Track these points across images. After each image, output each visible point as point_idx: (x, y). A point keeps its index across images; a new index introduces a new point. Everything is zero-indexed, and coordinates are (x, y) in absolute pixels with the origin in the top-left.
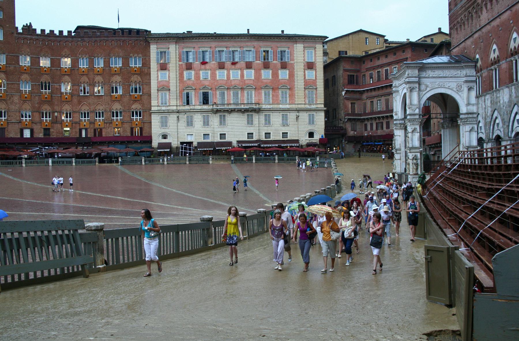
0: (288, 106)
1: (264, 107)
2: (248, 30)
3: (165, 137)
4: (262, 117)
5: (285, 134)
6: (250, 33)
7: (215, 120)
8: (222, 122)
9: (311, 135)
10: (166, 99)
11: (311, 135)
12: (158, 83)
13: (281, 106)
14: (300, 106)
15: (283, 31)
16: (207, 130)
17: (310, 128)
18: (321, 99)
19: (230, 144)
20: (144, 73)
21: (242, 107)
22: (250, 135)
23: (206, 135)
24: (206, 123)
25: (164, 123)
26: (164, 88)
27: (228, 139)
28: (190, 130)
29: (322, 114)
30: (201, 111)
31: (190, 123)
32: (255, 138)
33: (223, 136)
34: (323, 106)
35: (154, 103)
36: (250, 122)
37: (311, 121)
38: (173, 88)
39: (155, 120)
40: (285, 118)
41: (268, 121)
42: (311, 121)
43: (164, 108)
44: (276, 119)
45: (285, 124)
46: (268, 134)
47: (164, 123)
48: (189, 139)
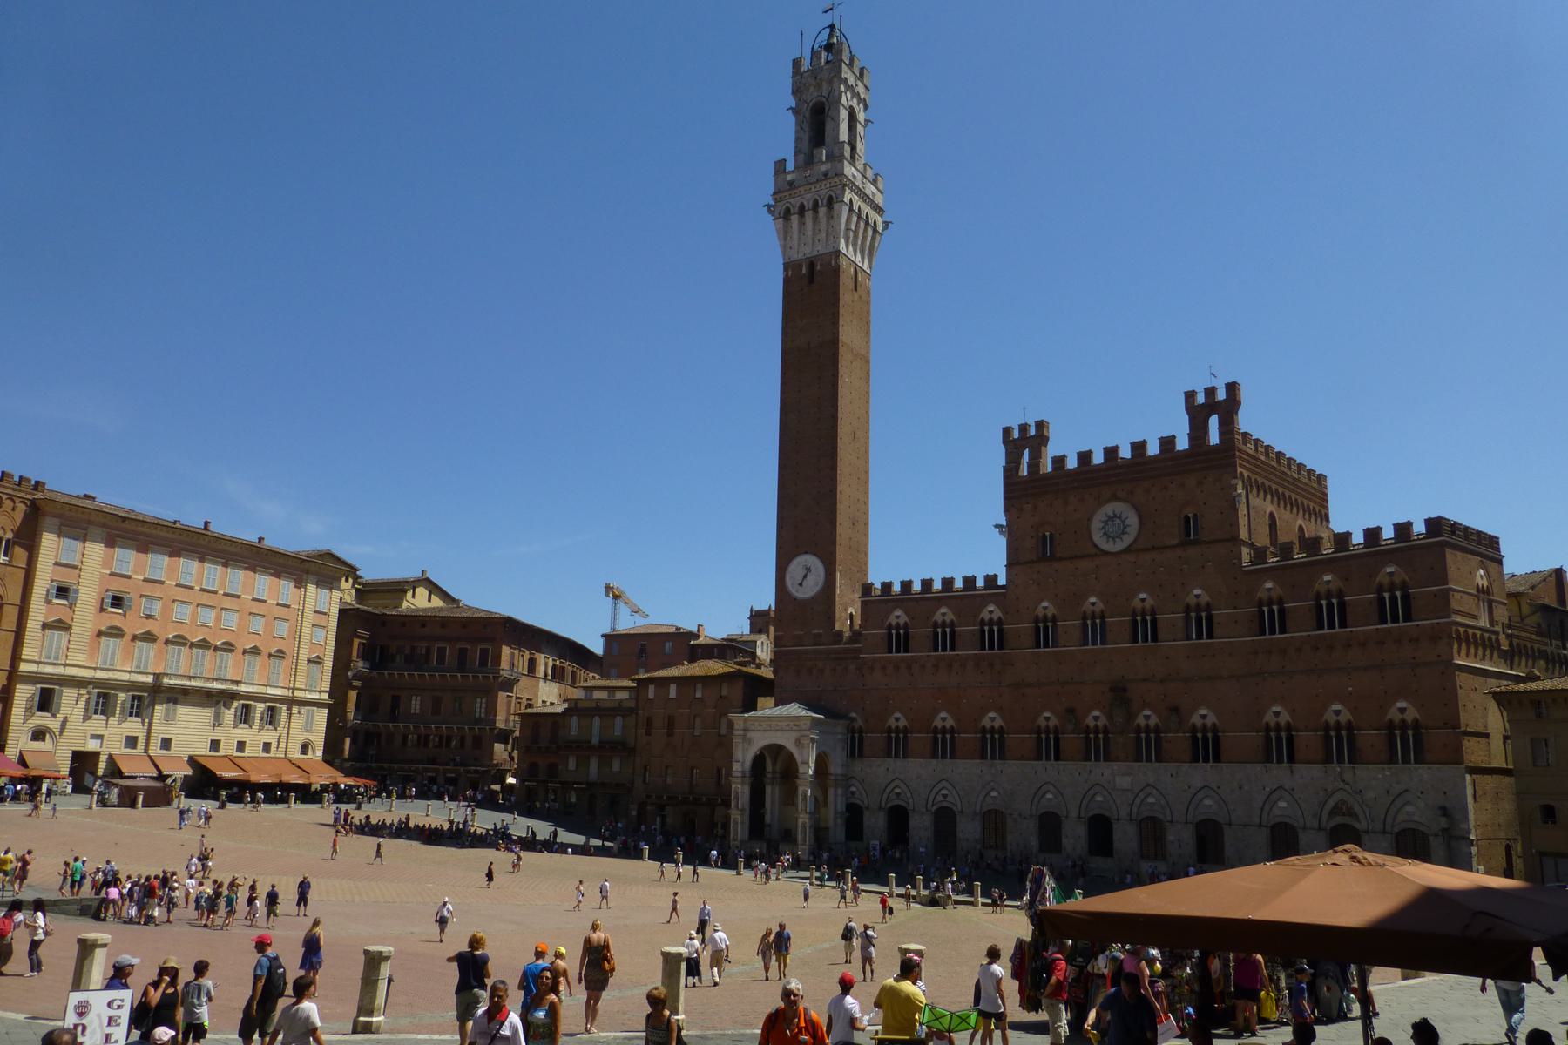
1: (243, 688)
2: (207, 523)
3: (39, 735)
6: (211, 527)
9: (305, 748)
10: (59, 648)
14: (297, 693)
15: (260, 540)
17: (307, 736)
18: (326, 686)
22: (215, 745)
23: (131, 742)
28: (97, 723)
29: (325, 711)
33: (166, 744)
34: (326, 696)
35: (28, 651)
37: (308, 726)
39: (23, 694)
42: (308, 726)
43: (49, 669)
47: (46, 702)
48: (92, 746)
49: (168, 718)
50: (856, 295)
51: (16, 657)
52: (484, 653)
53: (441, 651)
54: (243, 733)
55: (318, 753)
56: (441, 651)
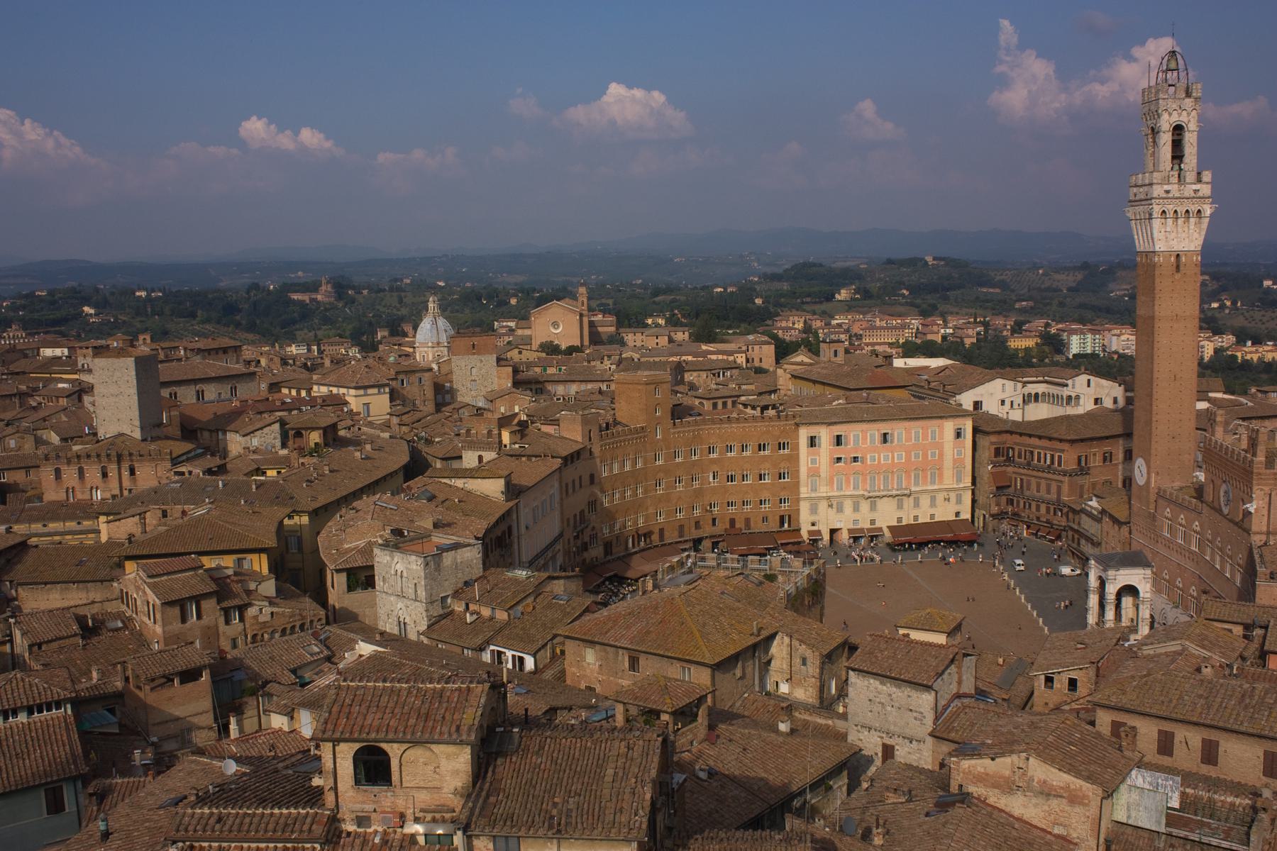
0: (936, 487)
1: (913, 489)
4: (911, 499)
5: (932, 516)
7: (865, 506)
8: (873, 508)
9: (957, 514)
11: (957, 514)
12: (809, 469)
13: (930, 488)
16: (857, 516)
17: (957, 508)
19: (880, 529)
20: (794, 459)
21: (894, 492)
22: (900, 520)
23: (856, 521)
24: (856, 508)
25: (814, 510)
26: (814, 473)
27: (878, 525)
30: (851, 496)
31: (840, 509)
32: (904, 523)
33: (873, 522)
36: (900, 507)
37: (959, 501)
38: (823, 475)
39: (804, 508)
40: (933, 499)
41: (917, 504)
42: (959, 501)
44: (925, 501)
45: (933, 503)
46: (916, 518)
47: (814, 510)
49: (873, 508)
50: (1177, 276)
51: (798, 493)
52: (1060, 457)
53: (1039, 454)
54: (916, 512)
55: (966, 515)
56: (1039, 454)
